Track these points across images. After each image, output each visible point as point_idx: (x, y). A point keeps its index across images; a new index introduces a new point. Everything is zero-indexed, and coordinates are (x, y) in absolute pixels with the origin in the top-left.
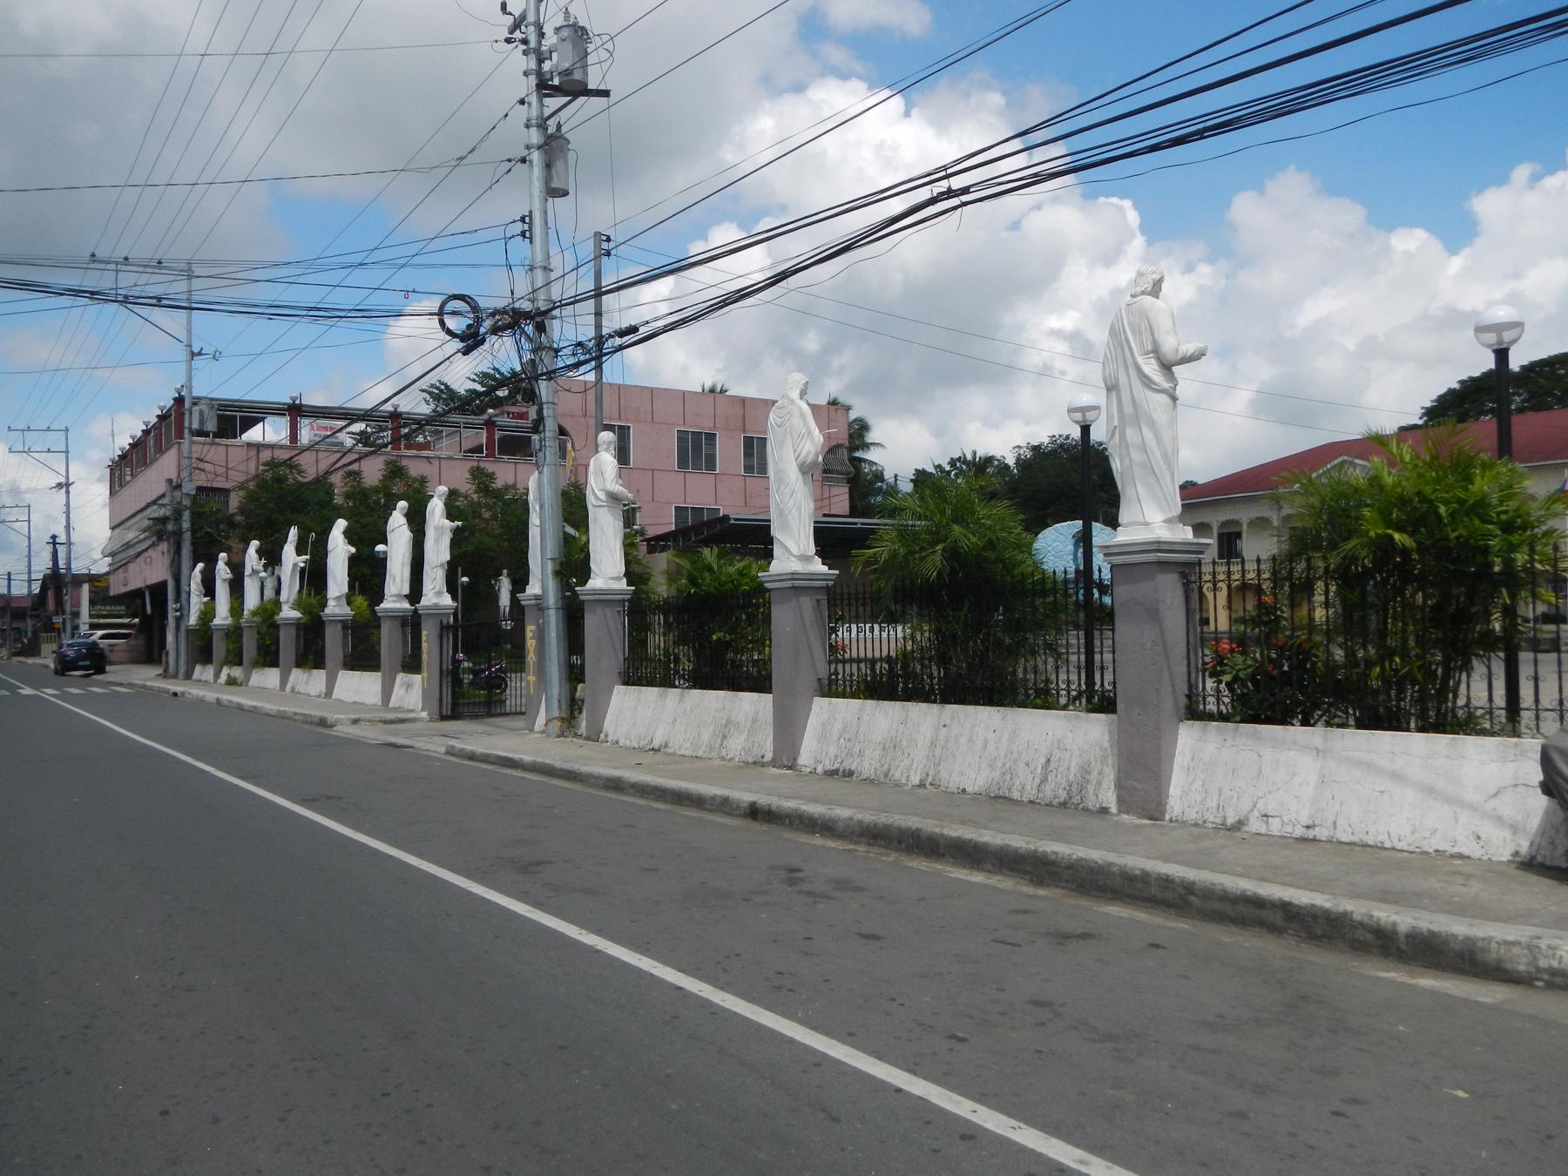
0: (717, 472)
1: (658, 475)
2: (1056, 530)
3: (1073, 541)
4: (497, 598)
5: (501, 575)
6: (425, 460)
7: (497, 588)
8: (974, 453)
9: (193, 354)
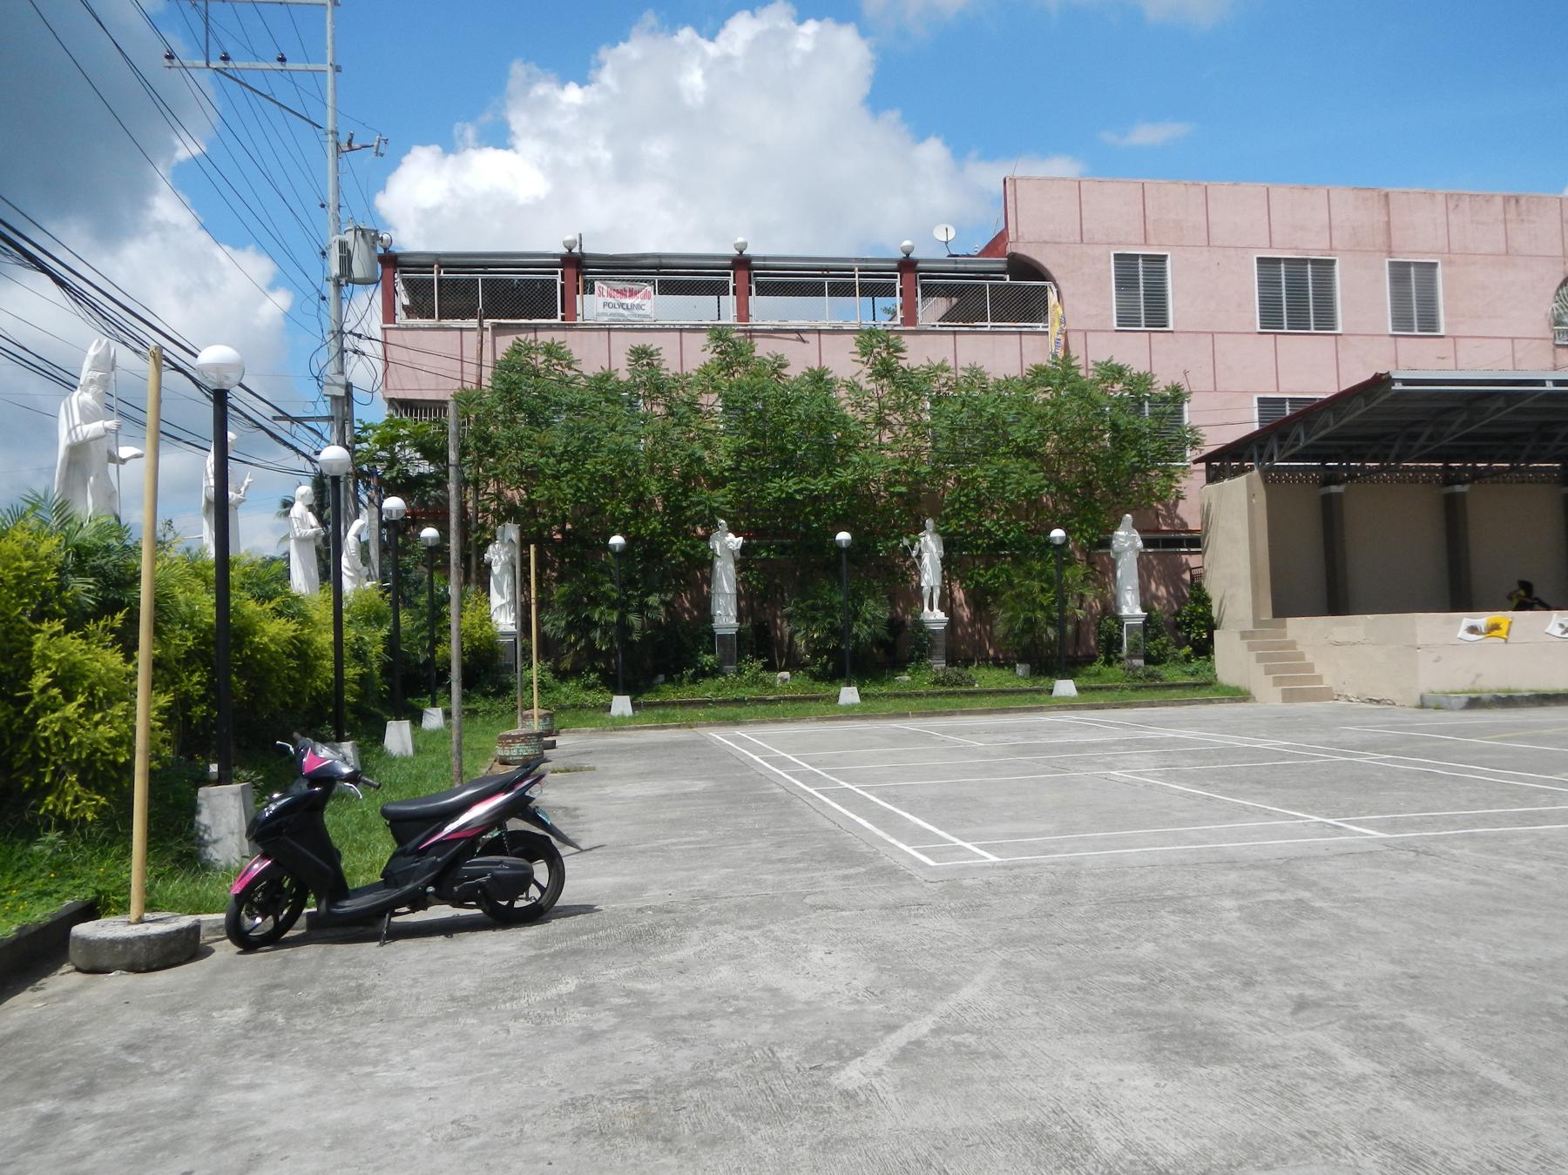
0: (1339, 331)
1: (1223, 343)
6: (795, 336)
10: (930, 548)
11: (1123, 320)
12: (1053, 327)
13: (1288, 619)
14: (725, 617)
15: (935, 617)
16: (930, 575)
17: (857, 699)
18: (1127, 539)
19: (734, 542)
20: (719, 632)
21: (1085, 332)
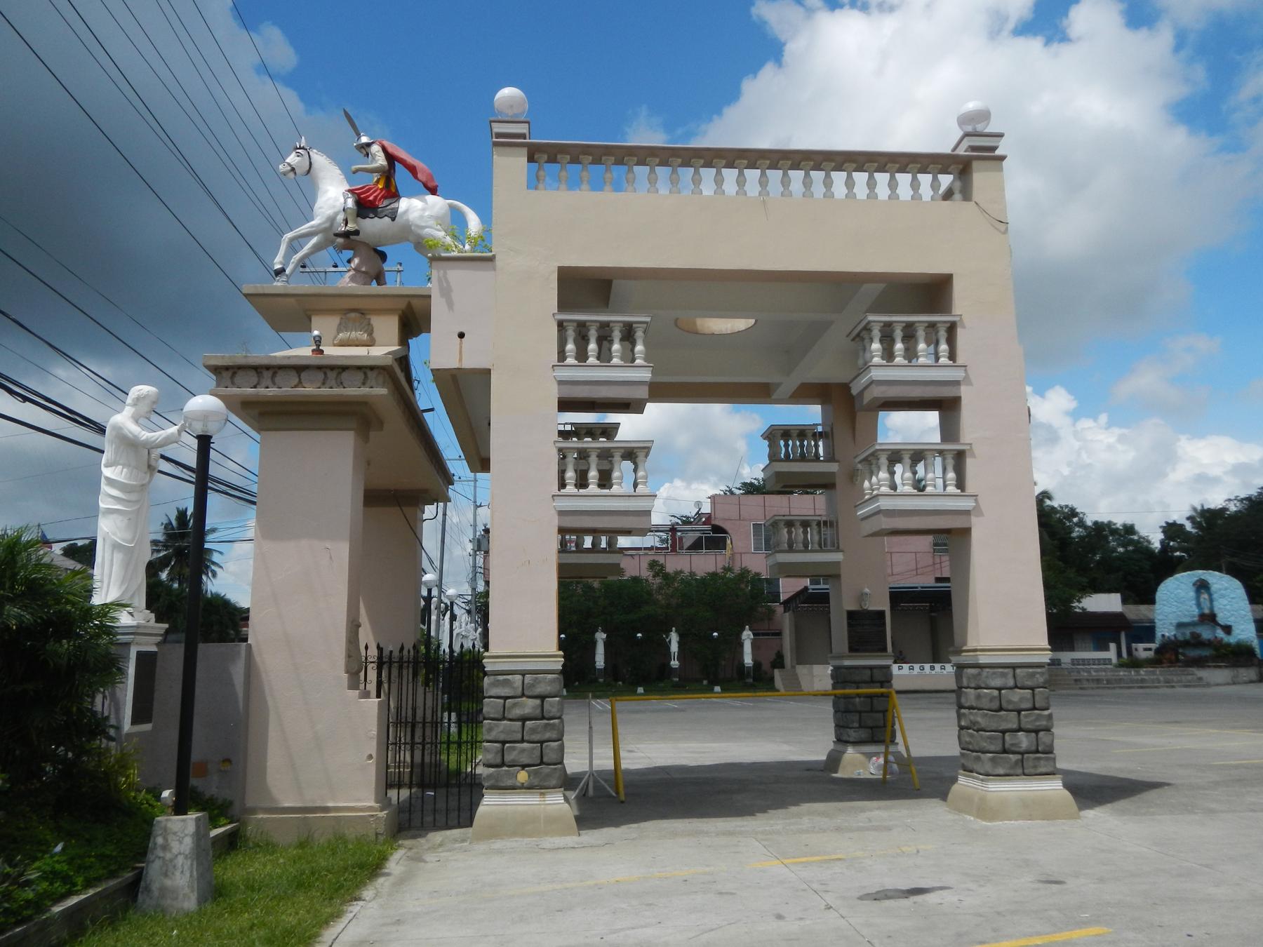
2: (1177, 579)
3: (1194, 589)
4: (668, 648)
5: (672, 631)
6: (630, 557)
7: (667, 640)
8: (1203, 506)
9: (477, 507)
10: (674, 639)
11: (756, 549)
12: (728, 552)
13: (815, 666)
14: (600, 661)
15: (675, 663)
16: (674, 647)
17: (642, 691)
18: (747, 635)
19: (604, 636)
20: (598, 667)
21: (741, 553)
